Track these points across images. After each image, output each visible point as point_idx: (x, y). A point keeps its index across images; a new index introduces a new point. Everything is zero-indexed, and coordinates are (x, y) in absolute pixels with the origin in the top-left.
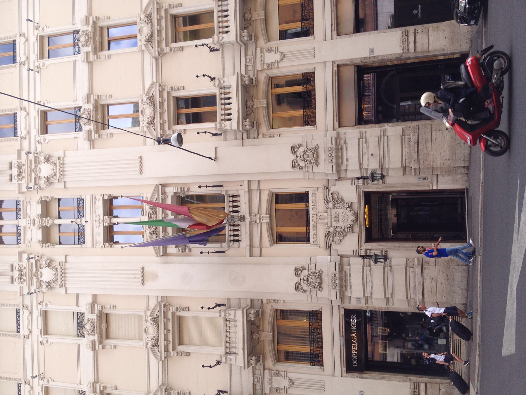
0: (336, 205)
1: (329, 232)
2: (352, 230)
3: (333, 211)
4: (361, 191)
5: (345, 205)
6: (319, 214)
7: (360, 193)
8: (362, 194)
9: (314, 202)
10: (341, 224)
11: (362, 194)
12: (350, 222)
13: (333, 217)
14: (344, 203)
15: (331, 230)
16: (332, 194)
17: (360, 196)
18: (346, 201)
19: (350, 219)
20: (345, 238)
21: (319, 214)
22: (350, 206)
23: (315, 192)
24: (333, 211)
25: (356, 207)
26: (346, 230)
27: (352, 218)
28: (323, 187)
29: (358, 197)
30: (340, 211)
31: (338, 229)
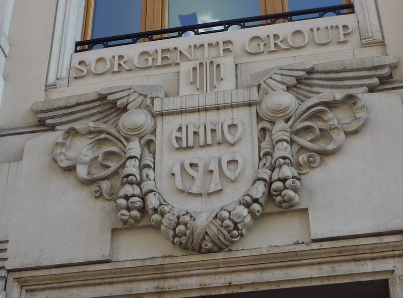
0: (281, 125)
1: (124, 109)
2: (127, 226)
3: (243, 116)
4: (388, 265)
5: (287, 171)
6: (227, 63)
7: (375, 254)
8: (369, 267)
9: (298, 41)
10: (168, 160)
11: (366, 269)
12: (179, 205)
13: (212, 116)
14: (298, 166)
15: (137, 118)
16: (350, 97)
17: (355, 256)
18: (315, 177)
19: (193, 205)
20: (84, 194)
21: (227, 63)
22: (276, 202)
23: (354, 39)
24: (243, 116)
25: (278, 235)
26: (128, 190)
27: (202, 214)
28: (389, 60)
29: (345, 247)
30: (247, 151)
31: (135, 148)
